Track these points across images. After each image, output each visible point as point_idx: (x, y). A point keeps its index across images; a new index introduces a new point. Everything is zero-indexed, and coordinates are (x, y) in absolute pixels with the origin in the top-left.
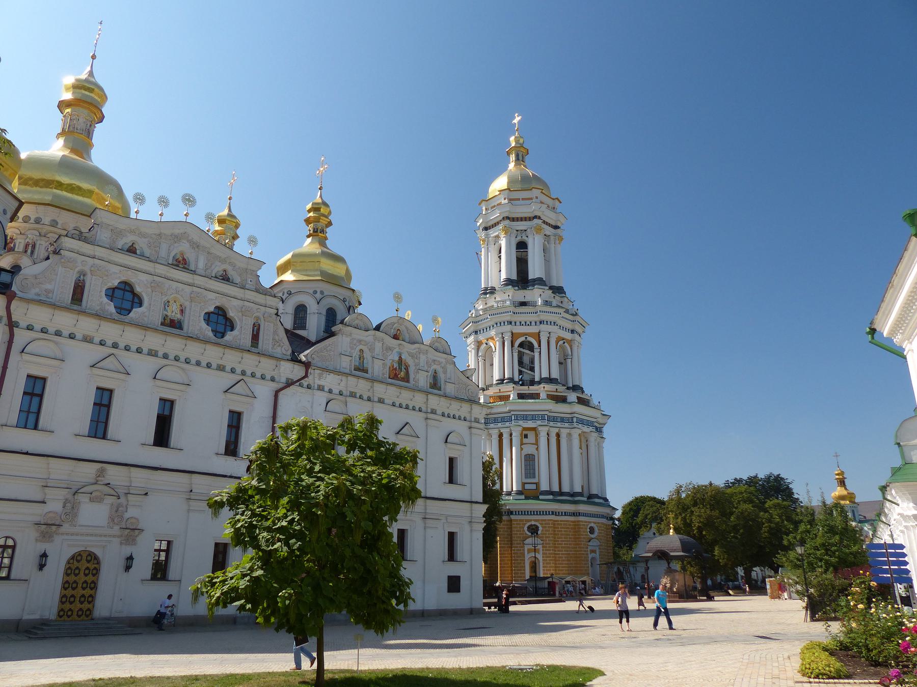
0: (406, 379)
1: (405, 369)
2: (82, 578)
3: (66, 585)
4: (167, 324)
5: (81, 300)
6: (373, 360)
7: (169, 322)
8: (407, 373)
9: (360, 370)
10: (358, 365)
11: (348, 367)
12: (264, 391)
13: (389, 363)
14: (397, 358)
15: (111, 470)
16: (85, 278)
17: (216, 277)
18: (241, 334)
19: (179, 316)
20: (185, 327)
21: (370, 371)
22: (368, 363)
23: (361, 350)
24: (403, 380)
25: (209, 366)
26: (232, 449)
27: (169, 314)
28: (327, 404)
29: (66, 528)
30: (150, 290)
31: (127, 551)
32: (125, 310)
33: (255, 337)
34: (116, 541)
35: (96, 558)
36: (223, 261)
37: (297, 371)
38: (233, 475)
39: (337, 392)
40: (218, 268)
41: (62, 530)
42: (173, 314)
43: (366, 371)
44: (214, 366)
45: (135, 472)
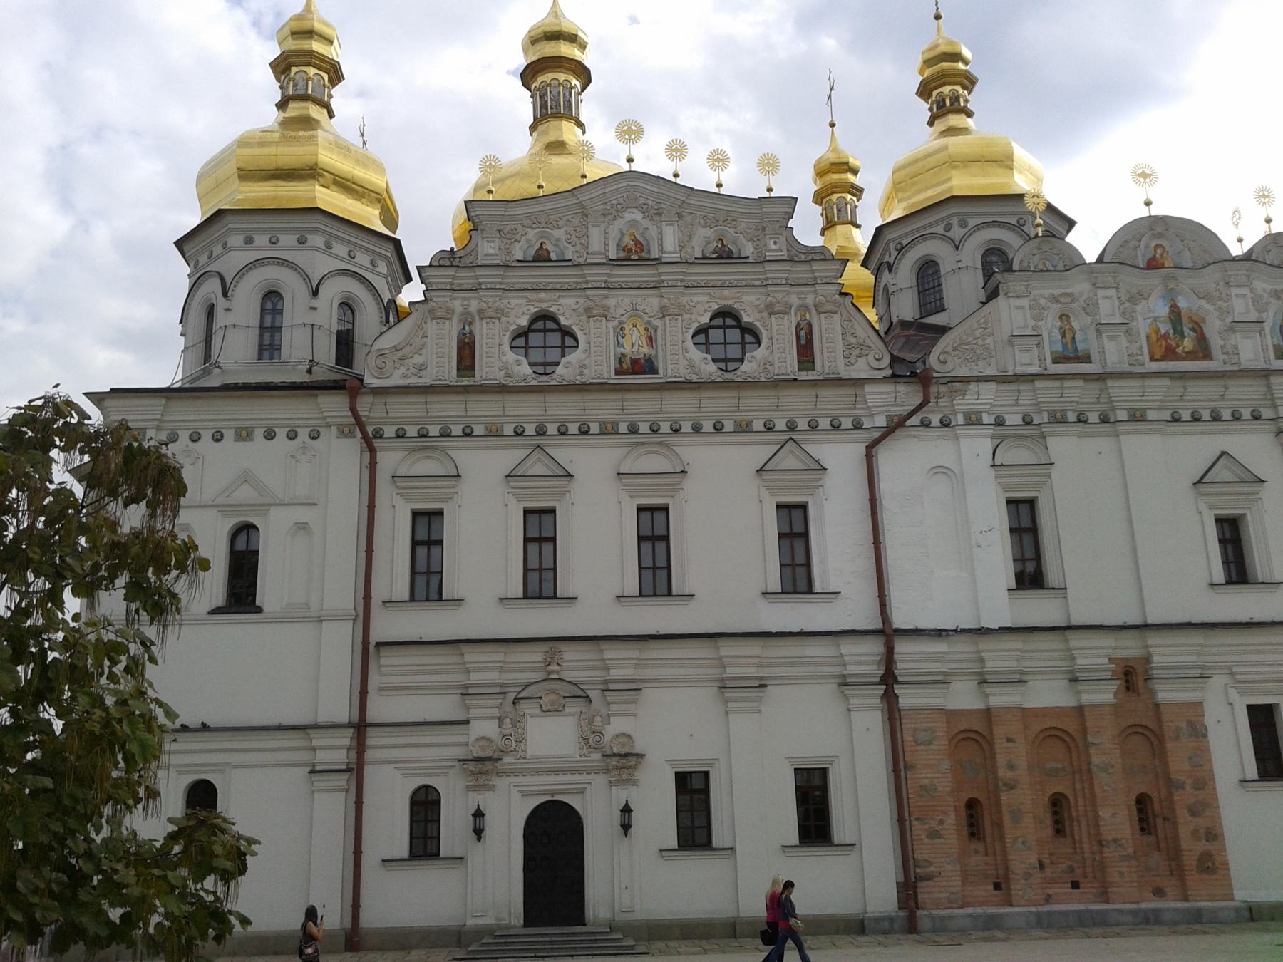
0: (1202, 350)
1: (1193, 330)
4: (627, 370)
5: (472, 367)
6: (1098, 331)
7: (628, 362)
8: (1202, 340)
9: (1070, 358)
10: (1060, 349)
11: (1037, 362)
14: (1163, 311)
15: (571, 654)
16: (473, 328)
19: (645, 350)
20: (661, 371)
21: (1095, 356)
22: (1087, 340)
23: (1064, 315)
24: (1191, 356)
25: (718, 429)
27: (627, 350)
28: (994, 454)
30: (584, 318)
31: (621, 795)
32: (545, 367)
33: (806, 351)
37: (905, 396)
39: (1017, 419)
40: (702, 239)
42: (635, 349)
43: (1087, 359)
45: (612, 653)
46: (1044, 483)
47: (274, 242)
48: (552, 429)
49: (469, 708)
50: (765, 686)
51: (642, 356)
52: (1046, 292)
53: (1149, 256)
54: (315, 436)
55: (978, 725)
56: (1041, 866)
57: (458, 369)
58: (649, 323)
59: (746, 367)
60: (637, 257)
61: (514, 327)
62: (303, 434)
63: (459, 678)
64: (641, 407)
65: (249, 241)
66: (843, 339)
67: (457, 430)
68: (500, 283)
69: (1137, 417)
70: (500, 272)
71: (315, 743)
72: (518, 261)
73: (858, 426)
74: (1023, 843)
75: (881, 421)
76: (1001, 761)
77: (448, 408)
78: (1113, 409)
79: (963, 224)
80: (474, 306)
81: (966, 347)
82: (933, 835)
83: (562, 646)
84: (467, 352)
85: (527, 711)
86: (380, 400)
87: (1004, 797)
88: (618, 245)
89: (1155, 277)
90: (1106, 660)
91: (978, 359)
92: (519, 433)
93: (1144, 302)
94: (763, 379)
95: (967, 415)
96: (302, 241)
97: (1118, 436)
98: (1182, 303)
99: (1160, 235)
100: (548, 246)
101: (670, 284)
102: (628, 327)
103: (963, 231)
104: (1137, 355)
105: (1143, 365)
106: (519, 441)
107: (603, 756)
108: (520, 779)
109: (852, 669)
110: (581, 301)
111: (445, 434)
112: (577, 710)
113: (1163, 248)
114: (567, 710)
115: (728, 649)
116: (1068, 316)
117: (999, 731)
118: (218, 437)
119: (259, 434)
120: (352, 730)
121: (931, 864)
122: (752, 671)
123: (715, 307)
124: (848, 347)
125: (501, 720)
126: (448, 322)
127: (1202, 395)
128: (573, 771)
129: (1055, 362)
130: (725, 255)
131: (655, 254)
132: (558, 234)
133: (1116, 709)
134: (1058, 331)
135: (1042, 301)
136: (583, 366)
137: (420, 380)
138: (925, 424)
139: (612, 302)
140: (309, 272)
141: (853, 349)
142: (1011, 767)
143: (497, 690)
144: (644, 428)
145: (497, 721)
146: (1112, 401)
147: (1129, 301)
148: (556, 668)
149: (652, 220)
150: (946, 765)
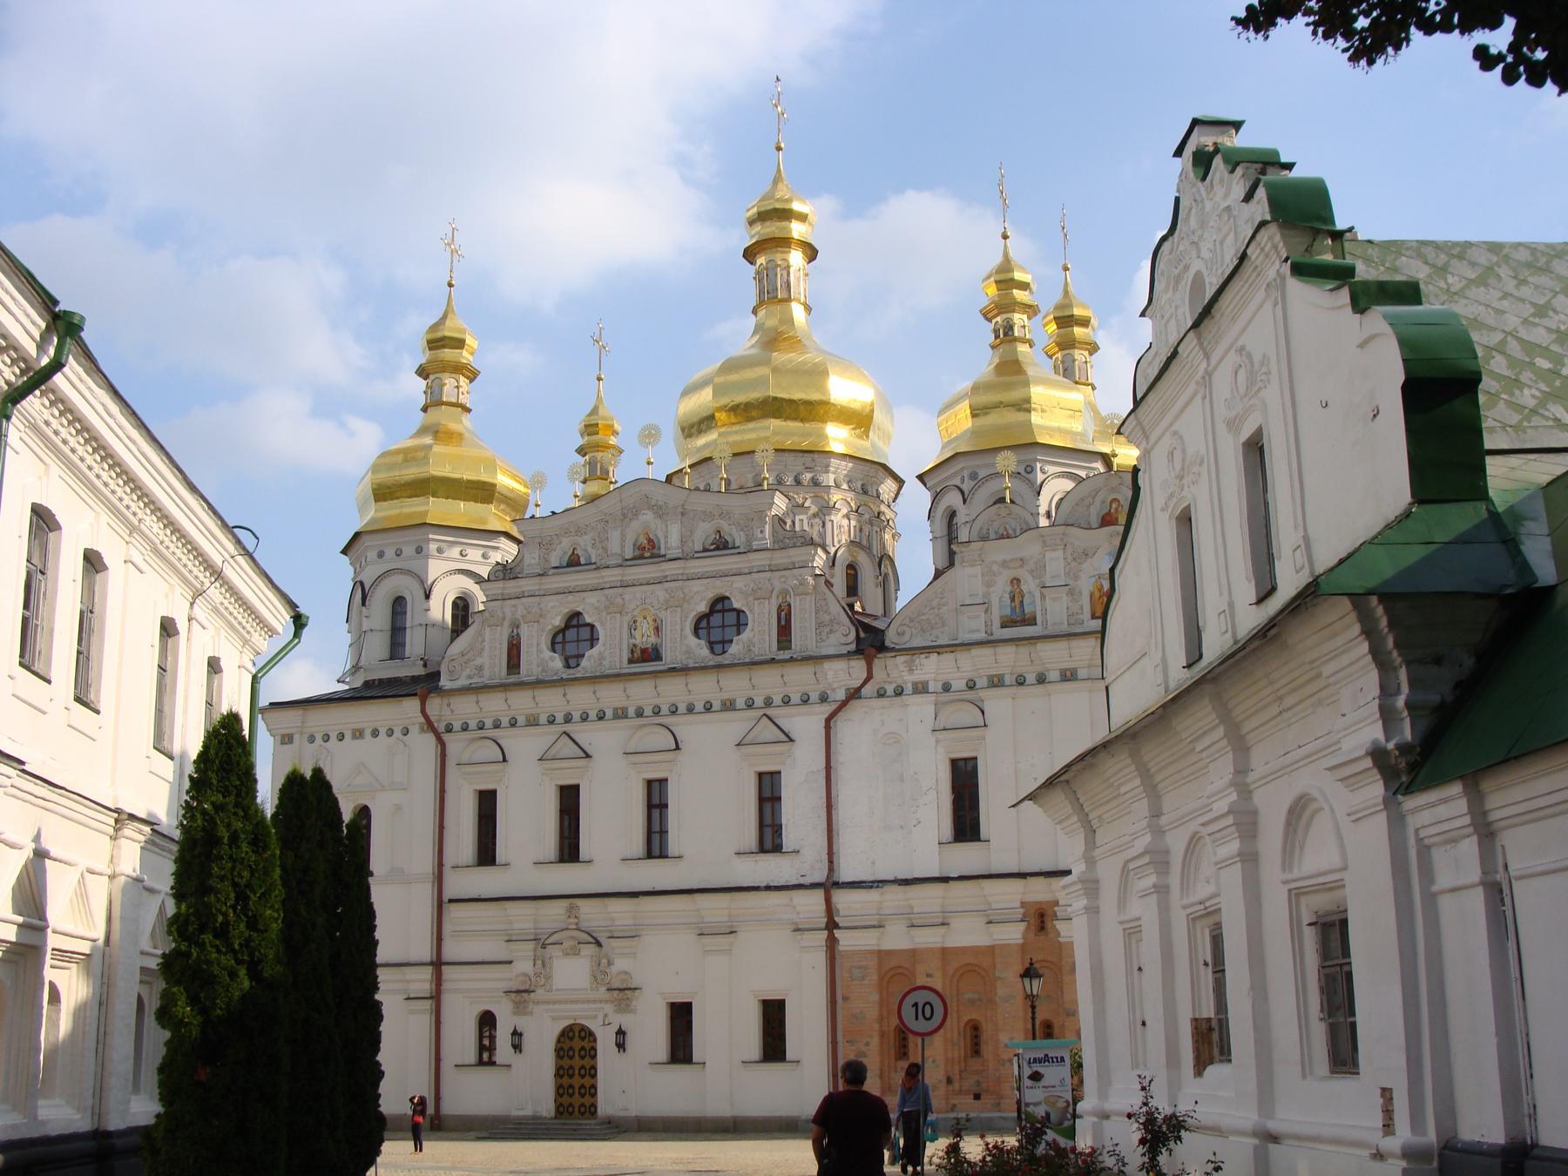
2: (577, 1062)
3: (560, 1072)
6: (1042, 594)
7: (639, 652)
9: (1016, 622)
11: (983, 628)
12: (806, 725)
15: (586, 907)
17: (705, 550)
18: (758, 635)
19: (653, 639)
21: (1039, 620)
23: (1015, 579)
25: (708, 708)
26: (770, 838)
29: (540, 994)
30: (604, 613)
33: (784, 631)
34: (609, 1008)
35: (591, 1034)
36: (707, 516)
37: (858, 667)
38: (772, 884)
40: (703, 533)
42: (644, 639)
44: (716, 705)
47: (399, 554)
48: (576, 716)
51: (649, 646)
52: (1000, 557)
53: (1103, 513)
54: (406, 732)
57: (508, 668)
59: (734, 649)
61: (550, 627)
62: (398, 733)
64: (642, 693)
65: (381, 555)
66: (816, 618)
67: (505, 721)
68: (539, 590)
69: (1068, 676)
70: (537, 580)
71: (408, 977)
73: (824, 699)
74: (933, 1062)
75: (841, 695)
77: (494, 705)
78: (1048, 671)
80: (520, 611)
81: (923, 617)
83: (579, 902)
84: (515, 652)
86: (445, 701)
88: (634, 545)
90: (1018, 905)
91: (932, 628)
92: (552, 721)
93: (1089, 560)
94: (747, 660)
95: (915, 685)
97: (1049, 695)
100: (578, 552)
103: (973, 483)
106: (553, 728)
108: (551, 1006)
111: (497, 725)
113: (1119, 501)
114: (582, 953)
116: (1018, 580)
118: (341, 737)
119: (368, 733)
120: (431, 968)
124: (820, 625)
126: (499, 628)
129: (1003, 626)
130: (721, 545)
131: (663, 552)
134: (1007, 597)
135: (995, 568)
136: (601, 658)
137: (479, 680)
138: (881, 694)
143: (532, 937)
144: (648, 711)
146: (1044, 664)
148: (576, 921)
150: (875, 997)
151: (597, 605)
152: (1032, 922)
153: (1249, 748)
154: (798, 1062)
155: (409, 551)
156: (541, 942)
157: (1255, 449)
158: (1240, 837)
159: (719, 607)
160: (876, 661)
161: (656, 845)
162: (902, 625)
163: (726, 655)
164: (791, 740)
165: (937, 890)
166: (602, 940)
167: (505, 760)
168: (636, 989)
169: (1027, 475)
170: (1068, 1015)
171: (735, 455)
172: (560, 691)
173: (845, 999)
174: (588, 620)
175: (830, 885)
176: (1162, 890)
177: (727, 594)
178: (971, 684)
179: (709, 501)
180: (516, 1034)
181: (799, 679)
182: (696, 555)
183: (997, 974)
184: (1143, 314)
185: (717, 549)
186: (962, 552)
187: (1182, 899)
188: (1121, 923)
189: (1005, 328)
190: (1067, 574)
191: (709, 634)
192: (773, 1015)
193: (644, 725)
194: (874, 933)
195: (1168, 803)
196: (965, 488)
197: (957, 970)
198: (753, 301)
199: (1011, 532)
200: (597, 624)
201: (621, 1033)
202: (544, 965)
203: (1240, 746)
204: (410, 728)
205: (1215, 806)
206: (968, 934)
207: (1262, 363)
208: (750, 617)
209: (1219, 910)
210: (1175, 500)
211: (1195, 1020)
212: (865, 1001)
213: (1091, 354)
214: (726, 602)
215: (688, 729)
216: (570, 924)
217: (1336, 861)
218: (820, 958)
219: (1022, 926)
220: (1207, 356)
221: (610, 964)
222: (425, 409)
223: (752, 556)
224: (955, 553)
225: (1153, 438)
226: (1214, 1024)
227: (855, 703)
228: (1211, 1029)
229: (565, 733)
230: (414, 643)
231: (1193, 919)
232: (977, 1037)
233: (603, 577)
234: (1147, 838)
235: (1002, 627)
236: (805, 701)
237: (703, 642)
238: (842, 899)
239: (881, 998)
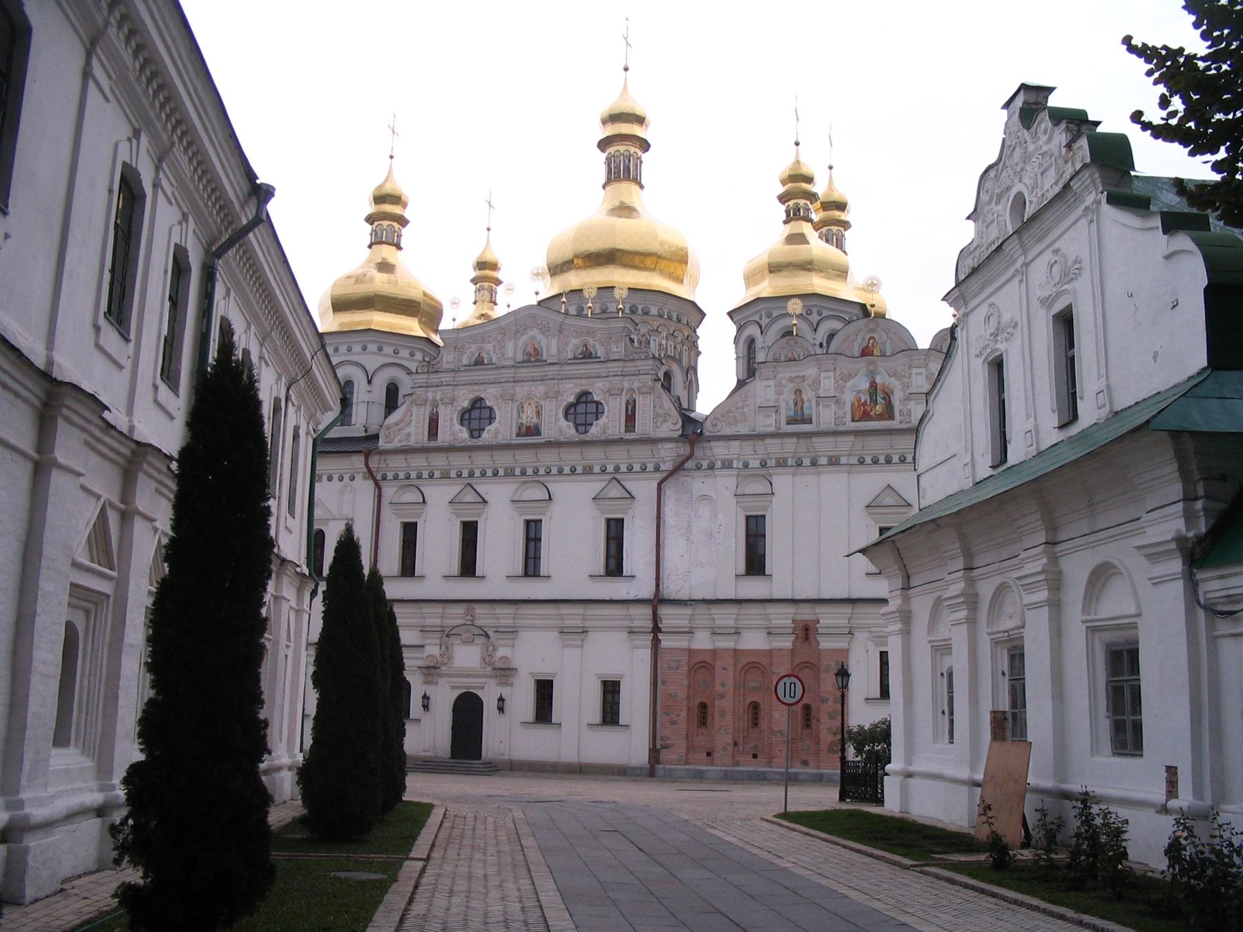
0: (889, 413)
1: (884, 398)
6: (817, 401)
12: (644, 489)
13: (849, 397)
15: (479, 610)
17: (575, 358)
19: (535, 420)
22: (810, 409)
24: (880, 417)
26: (614, 566)
27: (524, 421)
30: (500, 401)
32: (475, 432)
33: (630, 419)
37: (684, 450)
40: (574, 344)
41: (438, 671)
43: (810, 421)
44: (579, 470)
45: (501, 610)
46: (768, 506)
47: (349, 349)
48: (477, 473)
49: (425, 638)
50: (587, 632)
52: (787, 375)
54: (352, 479)
55: (708, 659)
56: (736, 744)
58: (538, 403)
60: (533, 359)
61: (460, 408)
62: (346, 478)
63: (420, 621)
64: (526, 459)
67: (425, 475)
69: (834, 462)
70: (452, 374)
72: (464, 366)
73: (657, 469)
74: (725, 730)
76: (718, 682)
77: (418, 461)
78: (819, 457)
79: (769, 315)
81: (731, 414)
82: (675, 723)
83: (474, 605)
84: (434, 424)
85: (457, 642)
86: (383, 457)
87: (717, 703)
88: (524, 352)
89: (862, 364)
90: (790, 622)
92: (459, 475)
93: (852, 380)
95: (723, 462)
96: (364, 348)
98: (879, 380)
99: (872, 330)
100: (484, 355)
101: (551, 377)
102: (526, 405)
104: (842, 417)
105: (845, 424)
106: (459, 481)
107: (494, 669)
108: (451, 680)
109: (636, 623)
110: (499, 390)
112: (480, 642)
114: (475, 642)
115: (565, 610)
116: (801, 392)
117: (718, 663)
121: (669, 739)
122: (578, 623)
123: (578, 390)
124: (656, 415)
125: (441, 645)
126: (423, 407)
127: (878, 446)
128: (475, 676)
130: (588, 355)
131: (544, 358)
132: (489, 347)
133: (793, 652)
135: (784, 382)
136: (497, 432)
137: (408, 444)
138: (699, 468)
139: (518, 389)
140: (367, 368)
141: (660, 417)
142: (723, 685)
143: (439, 629)
144: (530, 471)
145: (439, 647)
147: (842, 379)
149: (544, 334)
150: (685, 682)
151: (495, 394)
152: (800, 635)
153: (1056, 528)
154: (627, 726)
155: (357, 348)
156: (447, 634)
157: (1065, 321)
158: (1048, 589)
159: (584, 399)
160: (696, 445)
161: (532, 566)
162: (715, 419)
163: (588, 434)
164: (633, 497)
165: (733, 610)
166: (491, 634)
167: (424, 501)
168: (513, 669)
169: (807, 316)
170: (823, 701)
171: (599, 288)
172: (467, 454)
173: (663, 683)
174: (488, 404)
175: (658, 601)
176: (971, 622)
177: (590, 390)
178: (763, 463)
179: (581, 322)
180: (426, 697)
181: (641, 454)
182: (569, 362)
183: (773, 670)
184: (968, 218)
185: (584, 357)
186: (760, 369)
187: (987, 628)
188: (930, 642)
189: (794, 209)
190: (836, 389)
191: (575, 418)
192: (611, 689)
193: (526, 482)
194: (686, 637)
195: (979, 562)
196: (763, 323)
197: (744, 666)
198: (603, 180)
199: (796, 356)
200: (494, 407)
201: (501, 700)
202: (447, 647)
203: (1052, 527)
204: (356, 475)
205: (1027, 566)
206: (754, 641)
207: (1075, 262)
208: (606, 408)
209: (1023, 637)
210: (989, 350)
211: (993, 712)
212: (678, 685)
213: (845, 230)
214: (589, 396)
215: (557, 488)
216: (468, 620)
217: (1133, 611)
218: (646, 654)
219: (792, 638)
220: (1025, 252)
221: (495, 650)
222: (370, 247)
223: (610, 364)
224: (756, 369)
225: (971, 305)
226: (1009, 717)
227: (682, 473)
228: (1006, 719)
229: (468, 484)
230: (359, 415)
231: (996, 643)
232: (756, 714)
233: (500, 374)
234: (962, 585)
235: (787, 424)
236: (644, 470)
237: (571, 424)
238: (664, 611)
239: (689, 683)
